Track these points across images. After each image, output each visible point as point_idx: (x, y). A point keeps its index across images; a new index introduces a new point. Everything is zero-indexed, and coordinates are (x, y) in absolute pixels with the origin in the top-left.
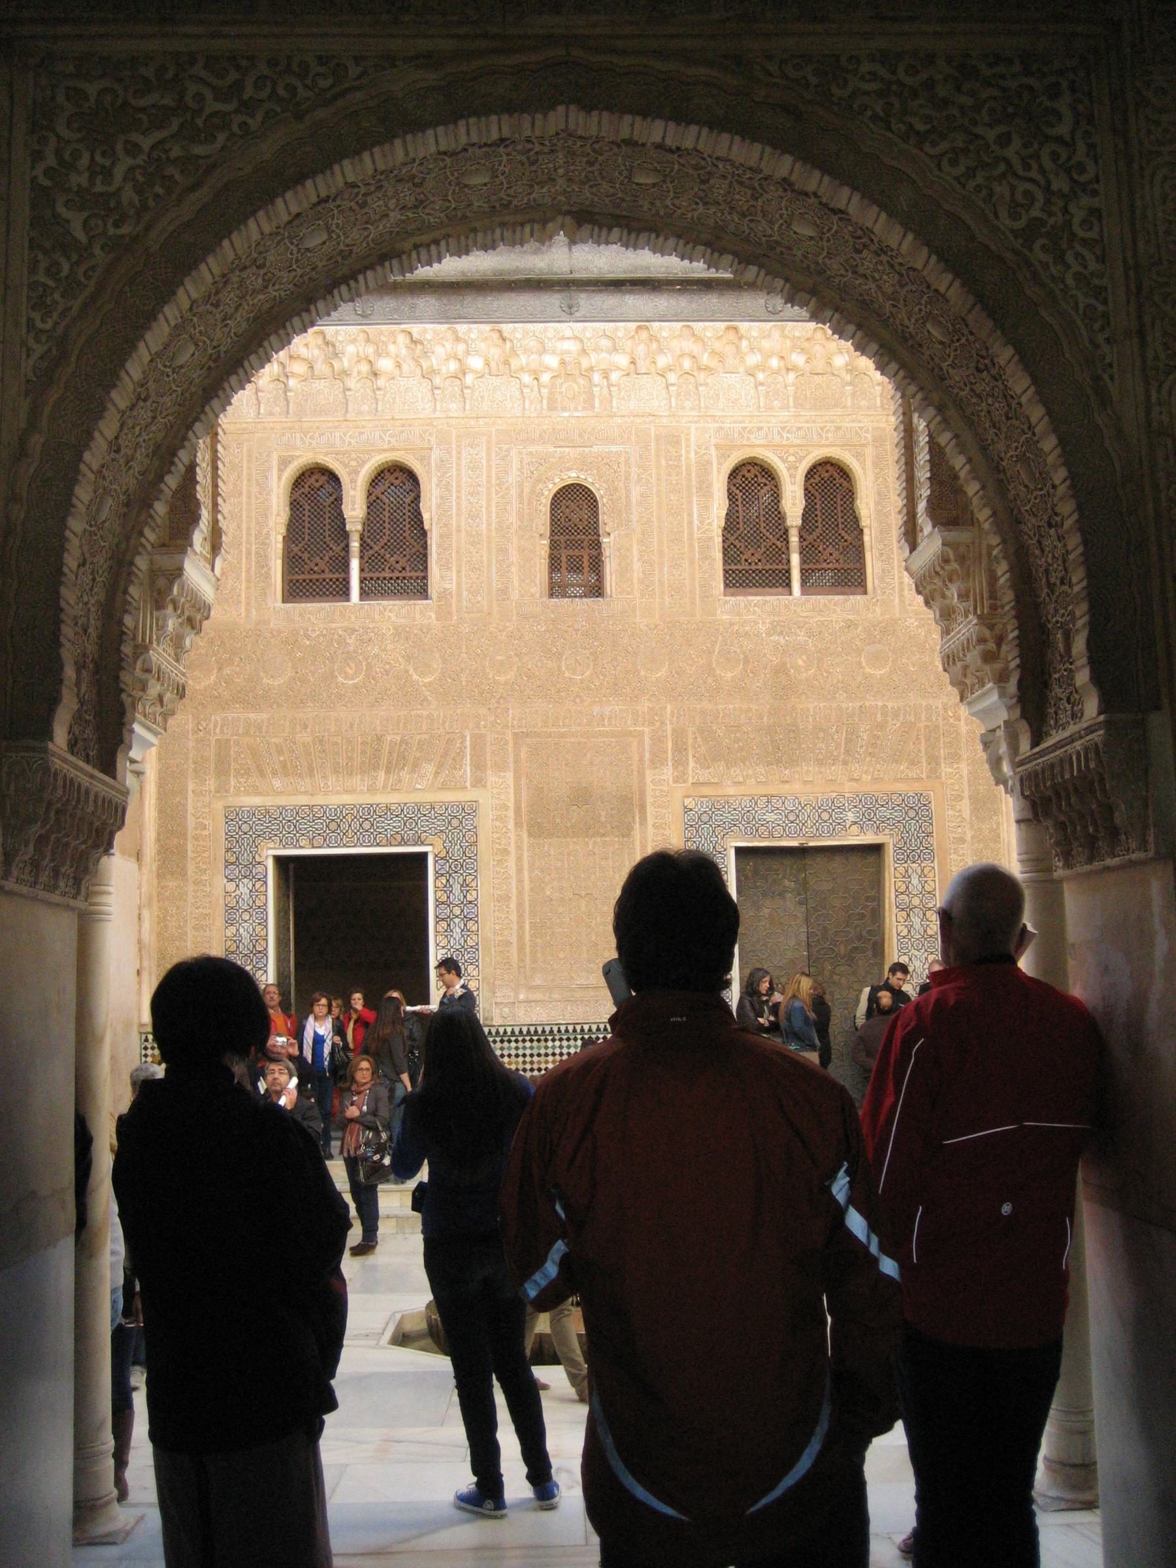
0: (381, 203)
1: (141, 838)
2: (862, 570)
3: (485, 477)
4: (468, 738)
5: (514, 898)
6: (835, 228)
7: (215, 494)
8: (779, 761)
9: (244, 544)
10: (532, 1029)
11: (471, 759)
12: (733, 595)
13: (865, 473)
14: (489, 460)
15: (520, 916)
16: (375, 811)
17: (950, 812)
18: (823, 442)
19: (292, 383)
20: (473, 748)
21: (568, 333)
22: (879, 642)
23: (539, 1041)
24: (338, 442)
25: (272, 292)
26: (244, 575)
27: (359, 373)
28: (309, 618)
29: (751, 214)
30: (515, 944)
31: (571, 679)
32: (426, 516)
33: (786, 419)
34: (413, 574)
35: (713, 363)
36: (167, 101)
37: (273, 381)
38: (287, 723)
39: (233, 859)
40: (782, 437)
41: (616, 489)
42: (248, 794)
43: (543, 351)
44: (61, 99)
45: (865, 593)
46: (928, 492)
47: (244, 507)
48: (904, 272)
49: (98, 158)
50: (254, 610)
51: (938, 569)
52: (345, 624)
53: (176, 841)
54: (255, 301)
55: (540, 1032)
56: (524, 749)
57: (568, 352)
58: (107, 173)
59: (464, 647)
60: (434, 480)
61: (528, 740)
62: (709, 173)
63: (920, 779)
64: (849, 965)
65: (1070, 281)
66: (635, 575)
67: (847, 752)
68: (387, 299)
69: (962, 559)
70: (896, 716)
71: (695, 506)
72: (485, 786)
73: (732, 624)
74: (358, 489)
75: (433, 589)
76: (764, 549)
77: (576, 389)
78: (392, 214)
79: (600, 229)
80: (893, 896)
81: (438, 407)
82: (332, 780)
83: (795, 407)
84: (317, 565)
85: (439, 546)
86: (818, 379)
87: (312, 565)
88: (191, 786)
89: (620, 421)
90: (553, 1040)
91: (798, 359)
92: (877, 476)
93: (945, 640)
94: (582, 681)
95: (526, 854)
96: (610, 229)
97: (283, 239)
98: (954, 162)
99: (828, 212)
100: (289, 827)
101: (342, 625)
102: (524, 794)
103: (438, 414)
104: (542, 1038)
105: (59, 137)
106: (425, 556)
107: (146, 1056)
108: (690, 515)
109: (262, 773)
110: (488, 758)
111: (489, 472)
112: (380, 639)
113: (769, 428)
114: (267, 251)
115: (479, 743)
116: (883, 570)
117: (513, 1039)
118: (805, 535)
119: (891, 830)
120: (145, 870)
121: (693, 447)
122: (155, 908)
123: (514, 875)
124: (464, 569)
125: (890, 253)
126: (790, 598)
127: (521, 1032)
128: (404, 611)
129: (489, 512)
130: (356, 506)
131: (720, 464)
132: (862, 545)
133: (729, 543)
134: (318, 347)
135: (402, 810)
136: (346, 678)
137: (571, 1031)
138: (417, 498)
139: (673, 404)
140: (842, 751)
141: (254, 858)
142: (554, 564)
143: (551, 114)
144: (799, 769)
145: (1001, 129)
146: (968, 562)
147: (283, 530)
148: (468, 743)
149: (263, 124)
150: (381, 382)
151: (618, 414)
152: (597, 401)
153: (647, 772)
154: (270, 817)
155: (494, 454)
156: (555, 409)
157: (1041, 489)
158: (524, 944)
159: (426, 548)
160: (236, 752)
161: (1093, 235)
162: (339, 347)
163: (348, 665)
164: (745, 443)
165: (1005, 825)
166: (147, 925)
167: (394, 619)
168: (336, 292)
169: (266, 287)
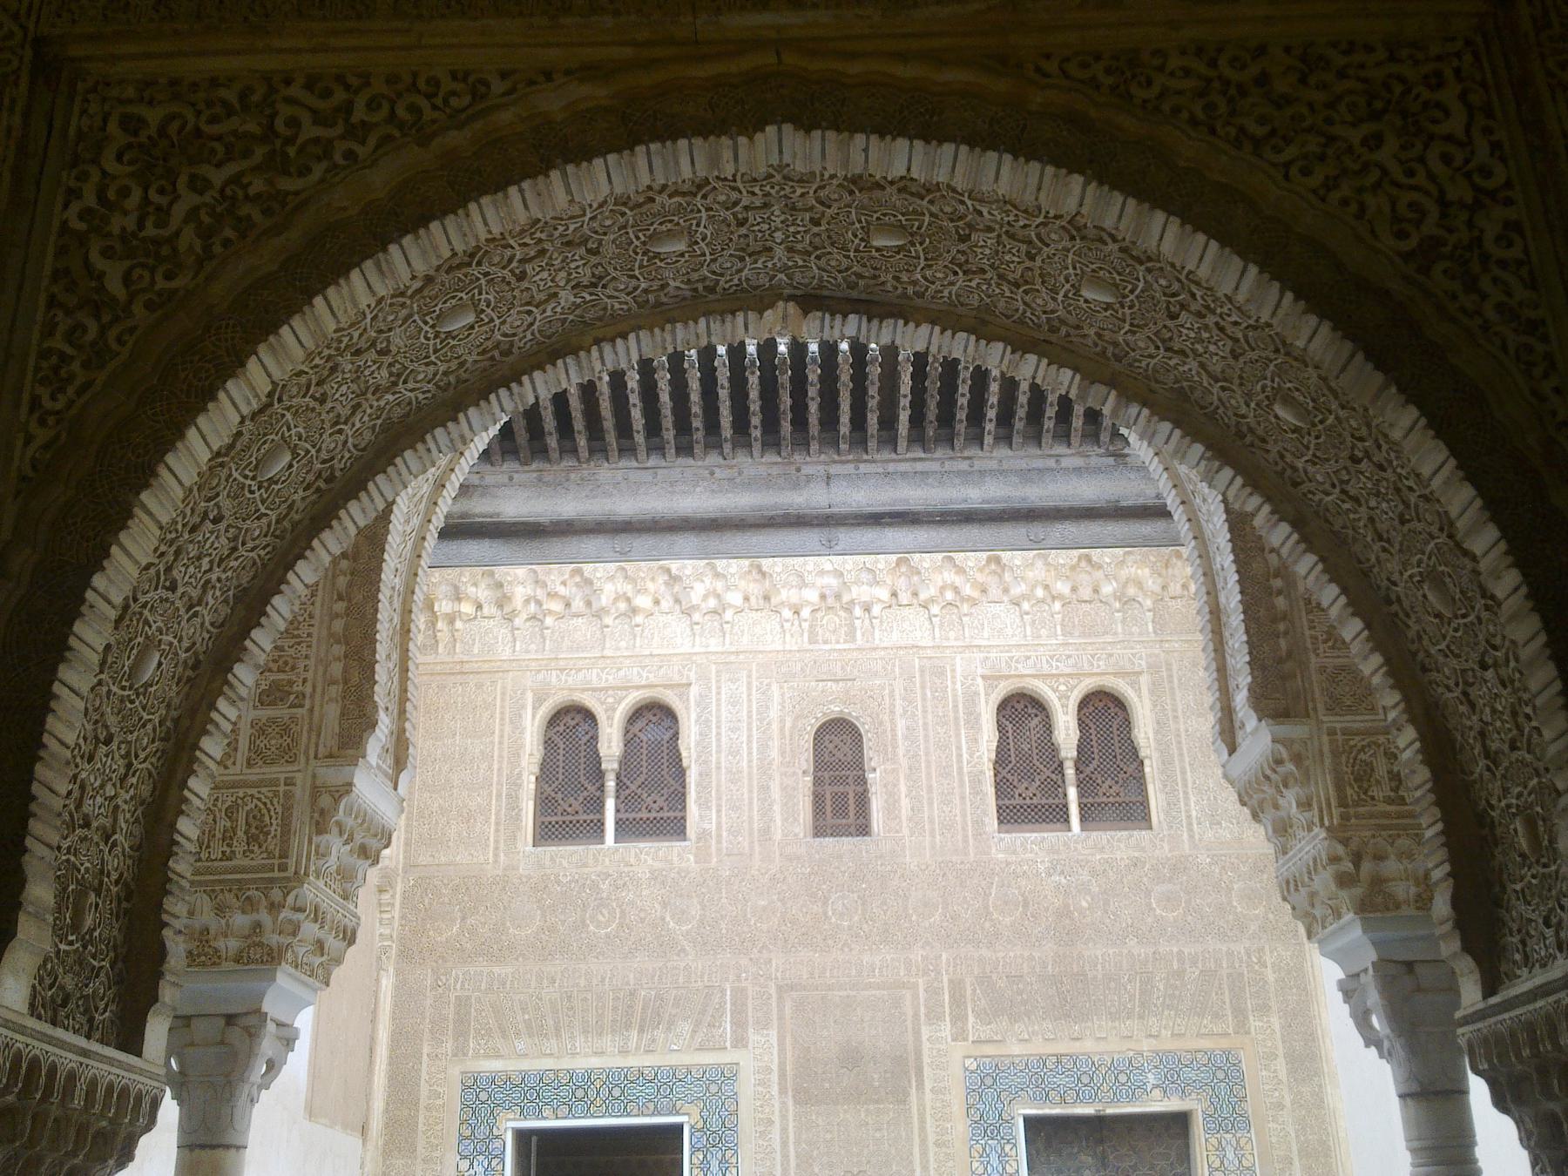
0: (545, 275)
1: (368, 1109)
2: (1145, 804)
6: (1141, 285)
7: (403, 698)
12: (1007, 832)
17: (1264, 1073)
18: (1095, 671)
19: (549, 621)
20: (733, 1004)
21: (828, 567)
25: (405, 392)
26: (493, 817)
27: (617, 610)
28: (561, 864)
29: (1027, 282)
32: (684, 754)
34: (671, 814)
35: (976, 594)
36: (252, 127)
39: (468, 1133)
41: (881, 723)
42: (487, 1057)
43: (803, 584)
44: (113, 127)
46: (1249, 679)
48: (1240, 335)
49: (153, 196)
51: (1268, 772)
52: (599, 868)
53: (406, 1112)
54: (382, 403)
56: (788, 1005)
57: (828, 586)
58: (163, 213)
60: (693, 716)
61: (794, 994)
62: (970, 226)
63: (1226, 1035)
65: (1490, 313)
66: (903, 811)
67: (1142, 1004)
69: (1297, 759)
70: (1194, 964)
73: (1008, 864)
74: (615, 726)
78: (562, 294)
79: (833, 315)
82: (580, 1041)
85: (698, 785)
86: (1086, 607)
87: (566, 807)
88: (426, 1050)
91: (1062, 587)
92: (1155, 706)
93: (1281, 862)
94: (850, 928)
95: (791, 1125)
96: (845, 316)
97: (410, 315)
98: (1306, 172)
99: (1130, 262)
102: (789, 1055)
103: (697, 649)
105: (104, 173)
106: (684, 794)
108: (959, 748)
110: (750, 1014)
111: (750, 706)
114: (390, 330)
115: (739, 994)
116: (1169, 804)
120: (370, 1146)
121: (959, 678)
123: (778, 1149)
125: (1219, 311)
126: (1070, 834)
132: (1143, 777)
133: (1000, 777)
134: (577, 584)
135: (656, 1075)
136: (597, 927)
138: (676, 736)
141: (491, 1130)
143: (759, 136)
144: (1089, 1024)
145: (1367, 128)
146: (1307, 763)
147: (536, 769)
148: (728, 998)
149: (374, 152)
150: (639, 619)
151: (882, 645)
156: (816, 642)
157: (1464, 616)
159: (684, 787)
161: (1515, 252)
162: (597, 584)
167: (650, 862)
168: (492, 397)
169: (395, 384)
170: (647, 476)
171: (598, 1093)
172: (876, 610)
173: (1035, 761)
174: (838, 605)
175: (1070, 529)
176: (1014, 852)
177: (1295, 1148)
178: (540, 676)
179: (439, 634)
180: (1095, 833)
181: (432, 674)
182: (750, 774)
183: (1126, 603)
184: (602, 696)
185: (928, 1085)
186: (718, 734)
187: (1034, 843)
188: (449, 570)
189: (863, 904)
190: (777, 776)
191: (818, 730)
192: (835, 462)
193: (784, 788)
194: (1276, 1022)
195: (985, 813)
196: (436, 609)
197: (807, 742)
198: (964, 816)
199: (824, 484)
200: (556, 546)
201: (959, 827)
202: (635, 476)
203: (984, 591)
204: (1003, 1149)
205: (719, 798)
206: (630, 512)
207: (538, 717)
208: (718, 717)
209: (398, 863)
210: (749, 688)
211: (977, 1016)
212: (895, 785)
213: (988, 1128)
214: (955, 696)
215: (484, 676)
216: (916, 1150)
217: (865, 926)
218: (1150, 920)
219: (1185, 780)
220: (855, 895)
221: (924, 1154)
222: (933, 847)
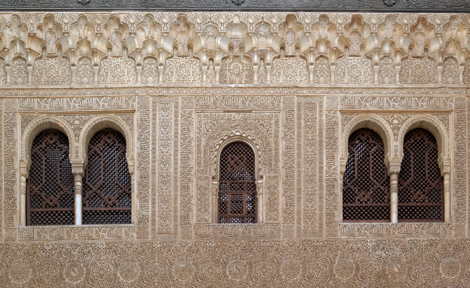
3: (173, 133)
14: (176, 121)
18: (419, 109)
19: (30, 59)
21: (236, 20)
33: (393, 91)
35: (342, 48)
40: (390, 105)
41: (268, 144)
50: (4, 230)
52: (71, 241)
59: (156, 258)
66: (280, 206)
71: (325, 156)
73: (348, 242)
75: (134, 218)
77: (241, 67)
85: (139, 184)
89: (272, 92)
103: (139, 84)
108: (321, 162)
111: (176, 129)
112: (96, 251)
113: (380, 98)
121: (325, 112)
124: (157, 202)
126: (390, 224)
128: (113, 232)
129: (176, 159)
130: (79, 155)
131: (343, 125)
136: (71, 280)
139: (311, 79)
147: (25, 171)
150: (96, 60)
151: (272, 85)
155: (180, 116)
156: (225, 82)
163: (73, 270)
164: (363, 109)
167: (106, 237)
172: (269, 58)
174: (242, 55)
176: (353, 235)
180: (407, 223)
182: (175, 178)
183: (446, 60)
184: (71, 118)
186: (154, 149)
189: (250, 268)
190: (194, 179)
193: (199, 188)
195: (335, 207)
198: (321, 210)
201: (317, 218)
205: (154, 195)
207: (26, 133)
208: (154, 136)
210: (176, 116)
212: (275, 188)
214: (321, 125)
217: (251, 282)
220: (245, 262)
222: (299, 231)
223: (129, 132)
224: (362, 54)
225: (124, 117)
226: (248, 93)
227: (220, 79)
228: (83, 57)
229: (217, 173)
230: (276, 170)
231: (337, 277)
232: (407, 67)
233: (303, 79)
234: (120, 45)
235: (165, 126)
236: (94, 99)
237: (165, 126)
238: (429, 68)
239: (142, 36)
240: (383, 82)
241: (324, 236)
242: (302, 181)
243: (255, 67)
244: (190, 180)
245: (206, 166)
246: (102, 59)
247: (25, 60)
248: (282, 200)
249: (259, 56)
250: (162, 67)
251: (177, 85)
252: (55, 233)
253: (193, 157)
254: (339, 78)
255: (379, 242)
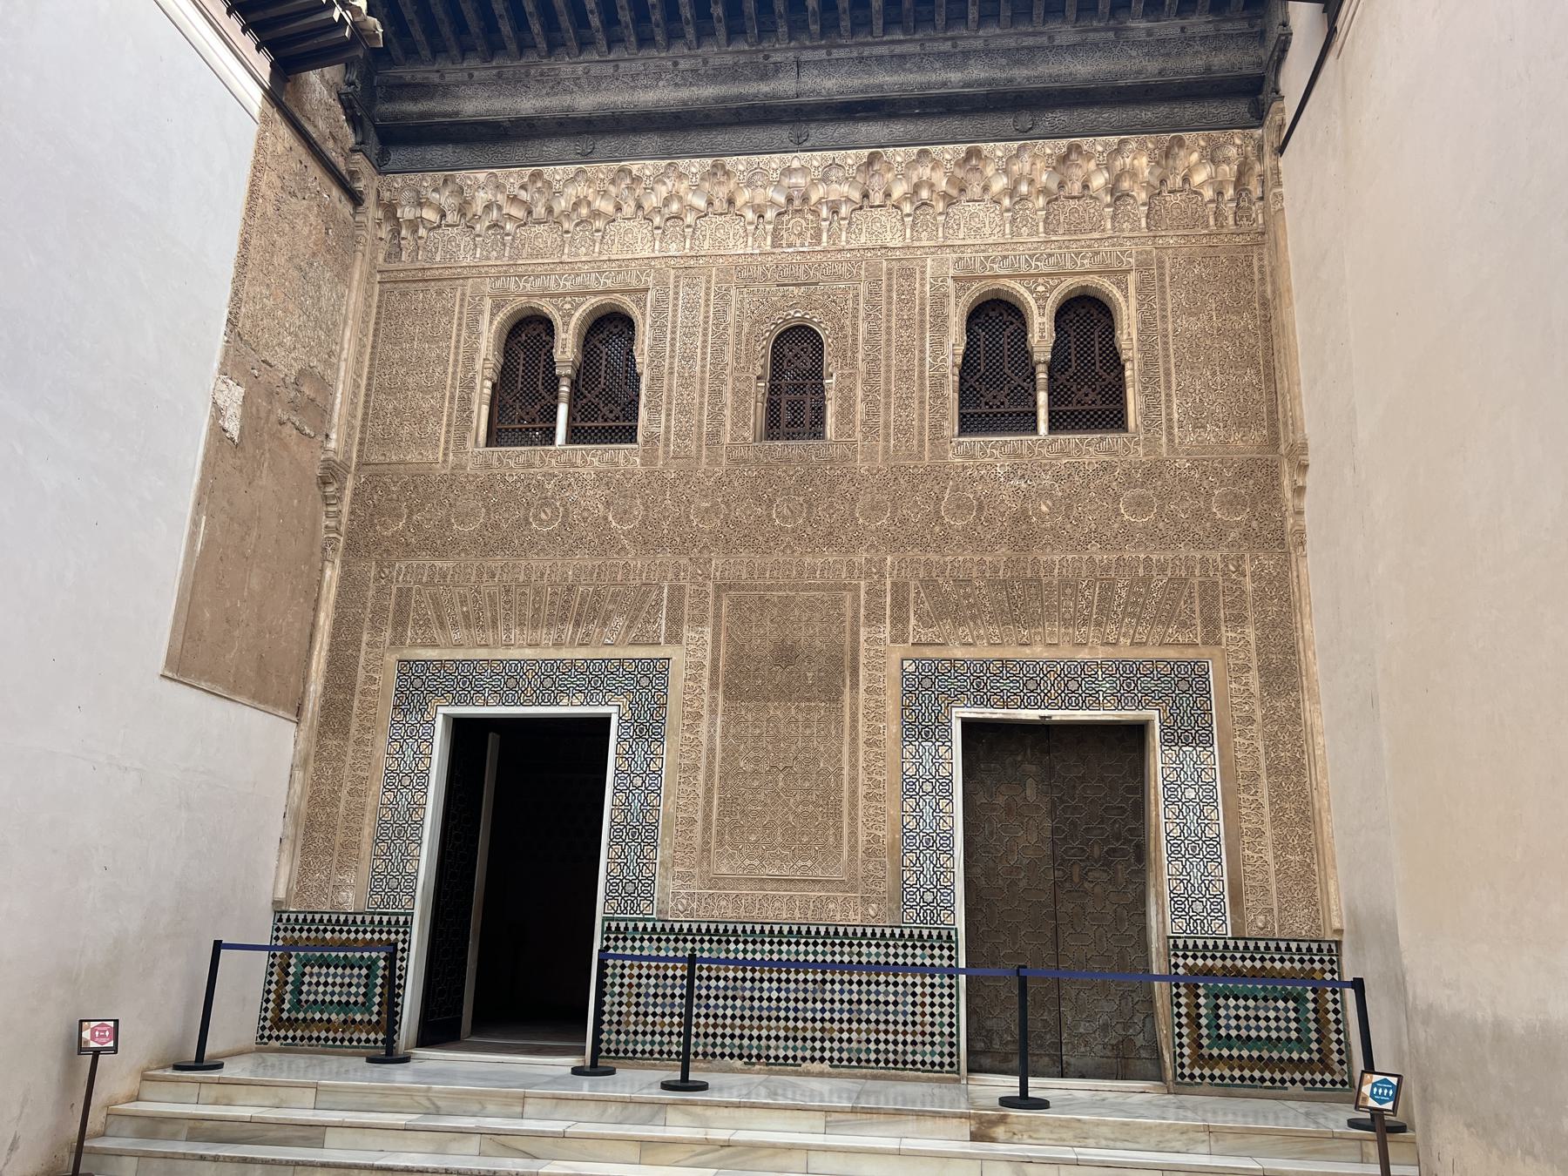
1: (304, 692)
3: (701, 317)
4: (666, 591)
5: (703, 769)
8: (1016, 621)
9: (448, 388)
10: (713, 927)
11: (667, 613)
13: (1127, 301)
14: (707, 300)
15: (709, 790)
16: (558, 668)
17: (1234, 685)
18: (1077, 269)
19: (509, 227)
20: (670, 601)
22: (1143, 485)
23: (719, 942)
24: (553, 285)
26: (445, 418)
27: (579, 215)
30: (700, 822)
31: (781, 528)
33: (1035, 245)
35: (954, 192)
37: (495, 225)
38: (474, 572)
42: (424, 646)
45: (1126, 430)
47: (453, 350)
52: (546, 469)
55: (721, 931)
56: (725, 602)
57: (796, 186)
60: (649, 321)
64: (1105, 871)
68: (608, 138)
70: (1163, 570)
72: (679, 642)
73: (964, 468)
74: (571, 332)
76: (1007, 391)
80: (1160, 786)
81: (657, 247)
82: (515, 632)
83: (1045, 233)
84: (528, 413)
85: (649, 388)
88: (365, 638)
89: (848, 255)
90: (737, 942)
100: (464, 683)
101: (540, 470)
103: (657, 254)
104: (724, 939)
107: (277, 938)
108: (922, 351)
109: (442, 625)
113: (1015, 256)
115: (677, 593)
116: (1148, 407)
117: (690, 938)
118: (1057, 375)
119: (1157, 704)
122: (311, 769)
126: (1034, 438)
127: (699, 930)
128: (607, 456)
129: (704, 353)
130: (566, 349)
133: (967, 385)
136: (539, 525)
137: (758, 932)
139: (908, 235)
140: (1095, 610)
142: (772, 408)
144: (1041, 630)
147: (488, 373)
148: (665, 595)
150: (599, 224)
151: (847, 247)
152: (825, 237)
153: (862, 629)
154: (445, 671)
156: (781, 246)
158: (710, 823)
160: (416, 602)
163: (544, 511)
164: (987, 273)
165: (1307, 703)
166: (297, 787)
167: (596, 464)
170: (609, 69)
171: (530, 683)
172: (844, 211)
173: (1006, 370)
175: (1060, 117)
177: (1263, 765)
178: (499, 283)
179: (402, 242)
181: (395, 282)
182: (702, 379)
183: (1118, 199)
185: (862, 687)
187: (996, 449)
188: (412, 176)
190: (730, 381)
191: (778, 338)
192: (806, 48)
193: (735, 393)
194: (1251, 633)
195: (944, 416)
196: (399, 215)
197: (764, 348)
198: (922, 419)
199: (794, 74)
200: (518, 151)
202: (595, 70)
203: (962, 190)
204: (937, 751)
206: (590, 108)
208: (674, 322)
209: (350, 458)
210: (707, 294)
211: (919, 618)
213: (921, 728)
215: (445, 283)
216: (846, 749)
217: (809, 529)
218: (1116, 526)
219: (1168, 382)
220: (801, 499)
221: (854, 753)
222: (886, 452)
223: (639, 317)
224: (986, 197)
225: (633, 297)
226: (813, 260)
227: (773, 242)
228: (582, 221)
229: (765, 371)
230: (853, 366)
231: (947, 520)
232: (1056, 212)
233: (896, 236)
234: (633, 204)
235: (691, 308)
236: (593, 275)
237: (691, 308)
238: (1092, 211)
239: (663, 191)
240: (1020, 235)
241: (927, 459)
242: (893, 378)
243: (825, 224)
244: (723, 382)
245: (748, 361)
246: (608, 223)
247: (502, 228)
248: (860, 407)
249: (830, 209)
250: (691, 230)
251: (710, 252)
252: (522, 459)
253: (730, 350)
254: (951, 231)
255: (1016, 467)
